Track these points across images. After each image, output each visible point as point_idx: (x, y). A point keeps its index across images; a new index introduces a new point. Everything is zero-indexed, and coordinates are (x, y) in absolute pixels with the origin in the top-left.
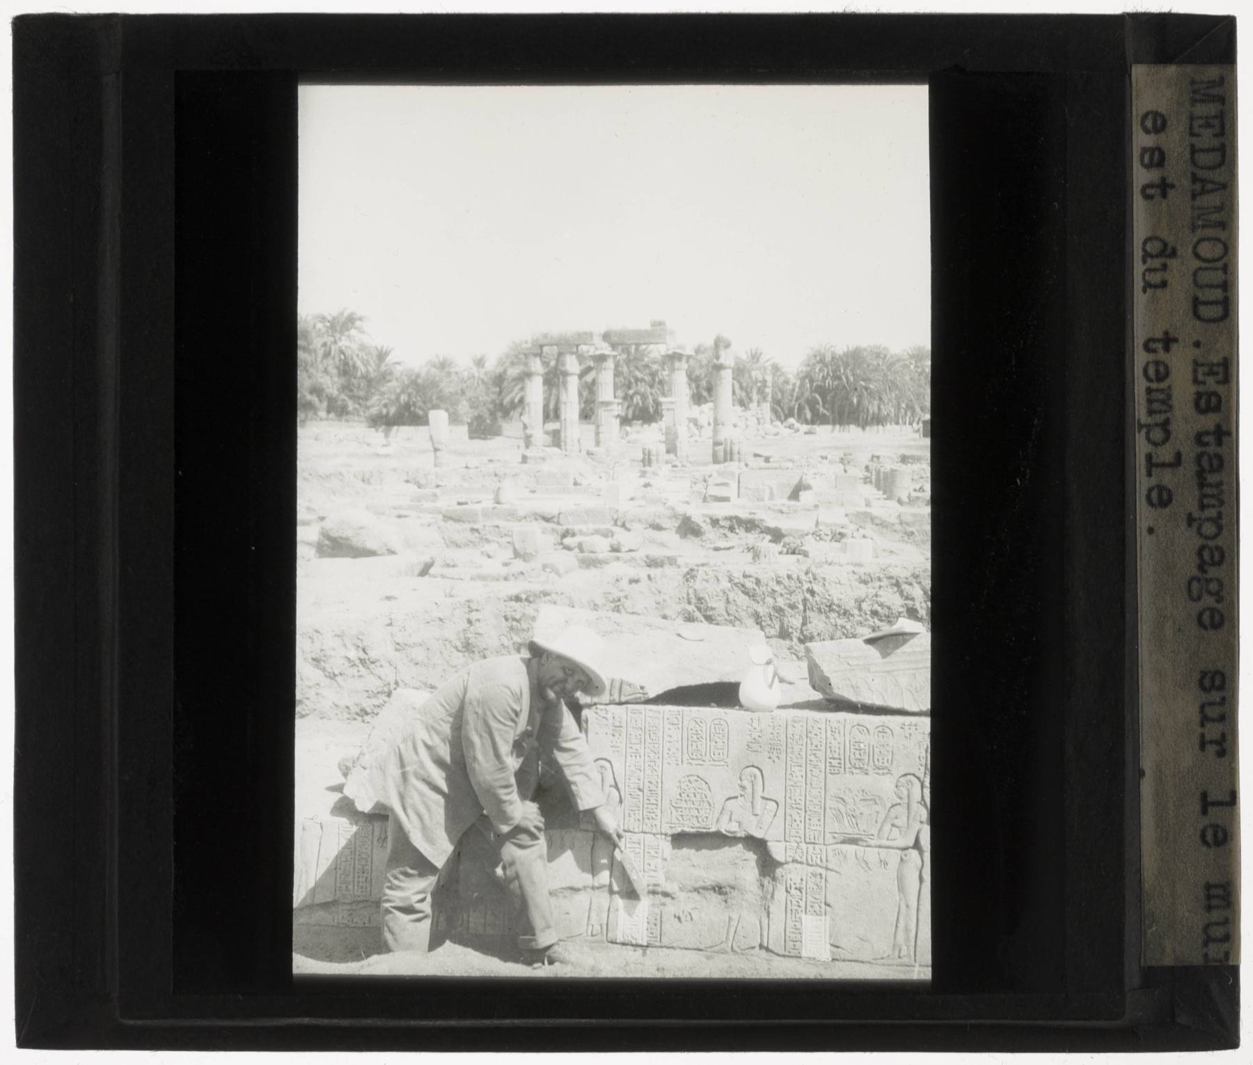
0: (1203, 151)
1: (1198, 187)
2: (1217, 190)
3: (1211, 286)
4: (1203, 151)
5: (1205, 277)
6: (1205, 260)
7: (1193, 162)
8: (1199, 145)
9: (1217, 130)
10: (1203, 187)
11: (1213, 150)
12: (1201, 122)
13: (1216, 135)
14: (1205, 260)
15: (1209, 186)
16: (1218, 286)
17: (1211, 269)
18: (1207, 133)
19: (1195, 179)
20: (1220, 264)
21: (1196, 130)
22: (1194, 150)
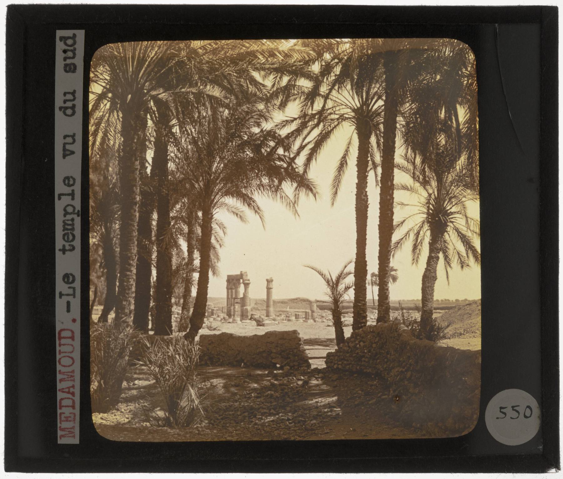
0: (71, 406)
1: (72, 390)
2: (63, 389)
4: (71, 406)
5: (70, 349)
6: (69, 357)
8: (71, 410)
9: (63, 416)
10: (69, 391)
11: (63, 406)
12: (69, 419)
13: (64, 413)
14: (69, 357)
15: (67, 390)
16: (64, 345)
17: (65, 352)
18: (67, 414)
19: (73, 394)
20: (62, 355)
21: (72, 416)
22: (73, 407)
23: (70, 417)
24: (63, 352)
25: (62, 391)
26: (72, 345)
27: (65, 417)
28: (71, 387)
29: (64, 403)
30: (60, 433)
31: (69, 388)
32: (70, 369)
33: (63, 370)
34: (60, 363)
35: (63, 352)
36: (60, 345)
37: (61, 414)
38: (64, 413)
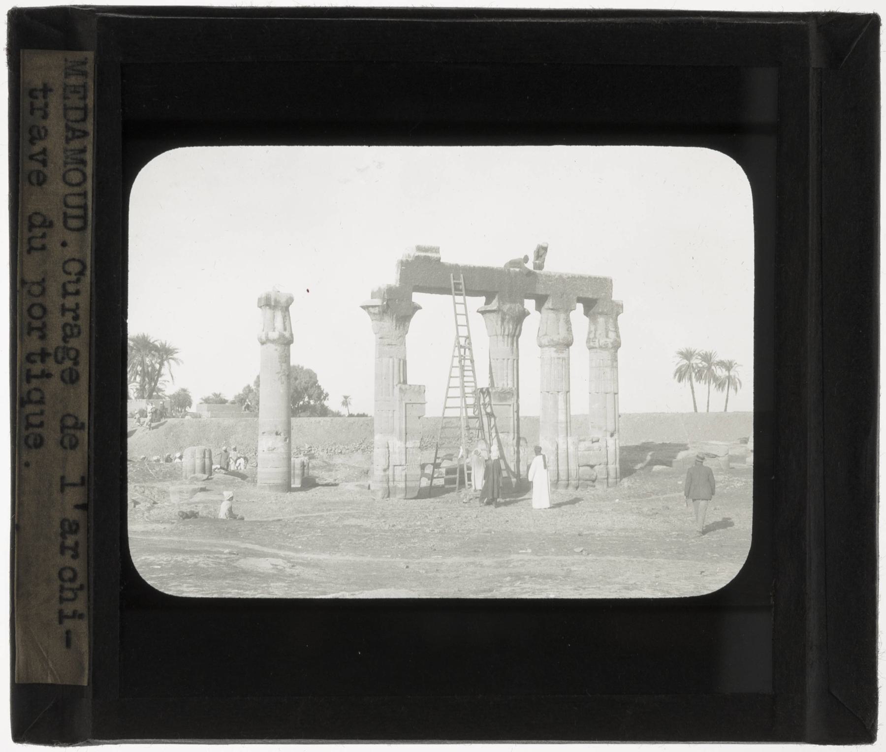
3: (73, 207)
4: (72, 108)
7: (65, 116)
8: (69, 103)
12: (73, 89)
22: (66, 109)
23: (71, 92)
24: (79, 195)
25: (85, 134)
26: (66, 205)
27: (78, 92)
28: (71, 139)
29: (78, 115)
30: (90, 68)
31: (73, 138)
32: (69, 167)
33: (81, 167)
34: (84, 175)
35: (79, 195)
36: (84, 207)
37: (84, 98)
38: (80, 98)
